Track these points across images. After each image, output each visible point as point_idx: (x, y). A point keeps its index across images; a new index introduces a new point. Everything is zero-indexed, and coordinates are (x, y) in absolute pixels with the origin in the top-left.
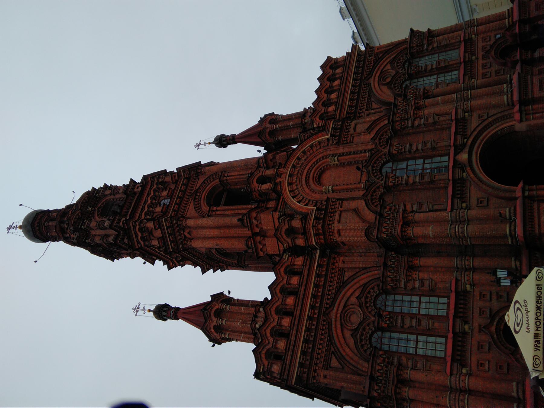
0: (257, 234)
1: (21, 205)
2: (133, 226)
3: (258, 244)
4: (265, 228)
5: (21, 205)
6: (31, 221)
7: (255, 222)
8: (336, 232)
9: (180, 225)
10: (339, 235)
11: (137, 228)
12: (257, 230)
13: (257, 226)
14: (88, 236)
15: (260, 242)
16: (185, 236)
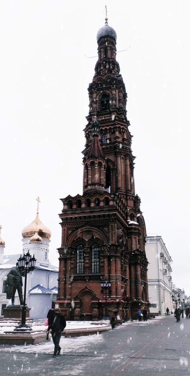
0: (127, 196)
1: (130, 46)
2: (125, 126)
3: (123, 196)
4: (128, 201)
5: (130, 46)
6: (115, 38)
7: (131, 198)
8: (135, 237)
9: (128, 156)
10: (134, 238)
11: (124, 127)
12: (128, 198)
13: (130, 198)
14: (116, 87)
15: (123, 197)
16: (122, 155)
